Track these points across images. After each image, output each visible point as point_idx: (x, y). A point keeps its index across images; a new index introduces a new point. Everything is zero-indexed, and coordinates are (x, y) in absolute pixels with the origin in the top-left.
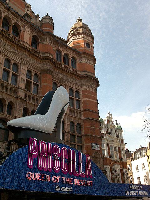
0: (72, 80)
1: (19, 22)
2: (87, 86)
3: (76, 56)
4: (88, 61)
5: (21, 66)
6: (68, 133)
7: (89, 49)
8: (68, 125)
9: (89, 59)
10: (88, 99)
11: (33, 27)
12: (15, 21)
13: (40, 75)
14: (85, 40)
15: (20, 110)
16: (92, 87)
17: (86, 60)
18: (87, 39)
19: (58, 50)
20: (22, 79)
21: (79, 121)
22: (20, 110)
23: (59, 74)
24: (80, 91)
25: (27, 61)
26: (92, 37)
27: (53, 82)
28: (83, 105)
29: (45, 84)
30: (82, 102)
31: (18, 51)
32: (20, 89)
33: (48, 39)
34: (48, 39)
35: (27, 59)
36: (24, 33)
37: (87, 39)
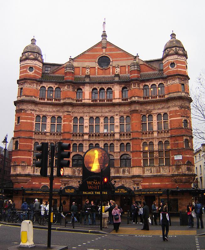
0: (159, 107)
1: (110, 86)
3: (163, 82)
6: (156, 151)
8: (156, 145)
11: (119, 83)
12: (107, 88)
13: (130, 116)
14: (170, 61)
15: (117, 147)
17: (171, 82)
19: (145, 85)
20: (116, 126)
21: (166, 139)
22: (117, 147)
23: (146, 108)
27: (142, 116)
29: (133, 122)
31: (111, 108)
32: (115, 134)
33: (133, 84)
34: (133, 84)
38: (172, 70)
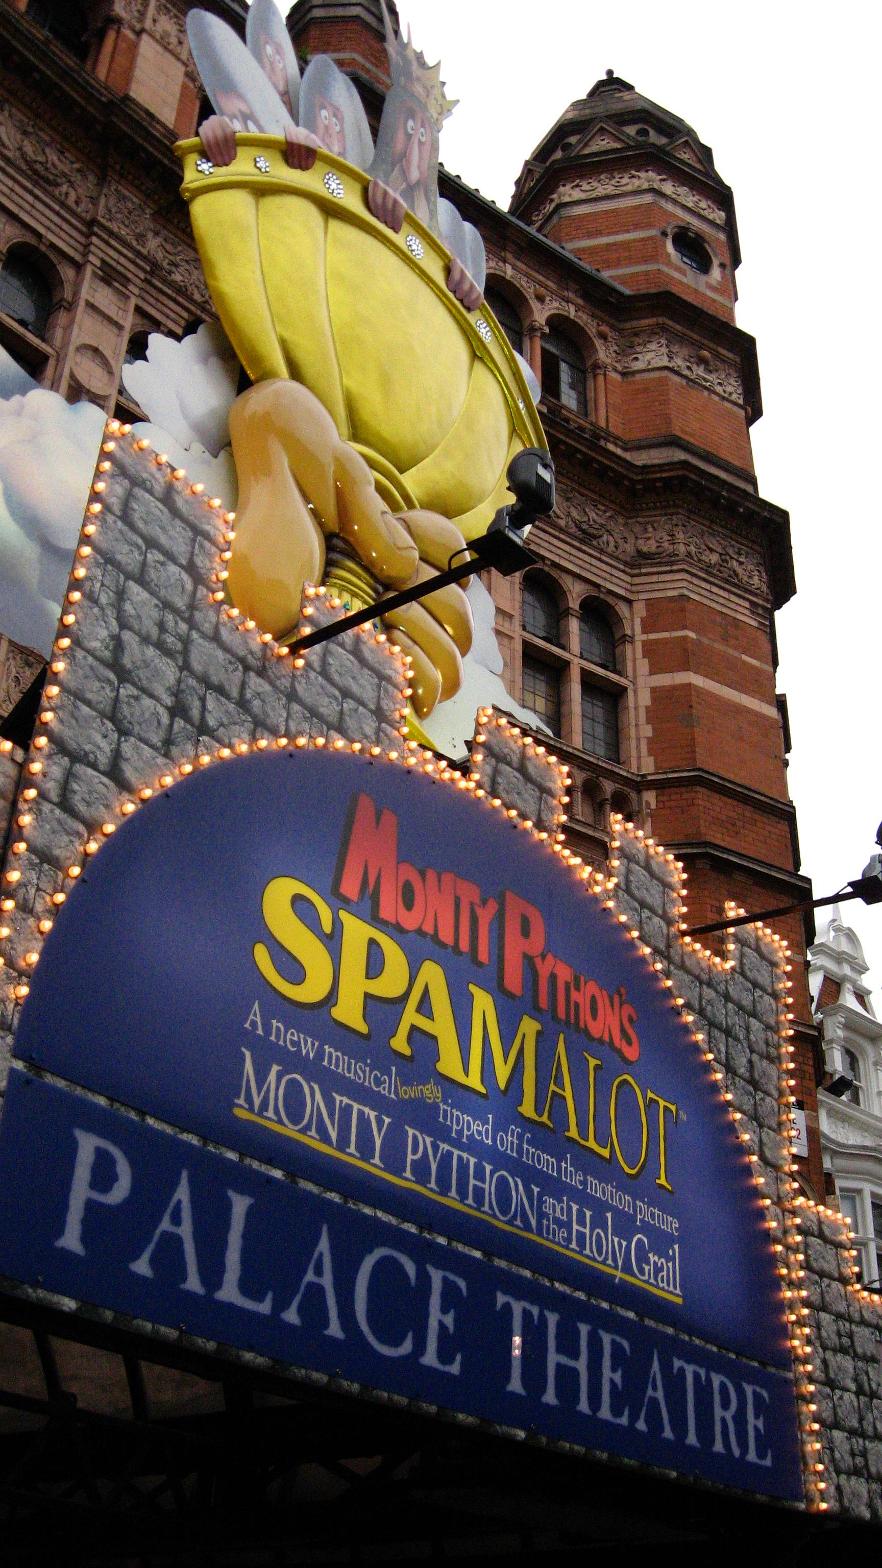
2: (687, 574)
4: (700, 371)
5: (77, 285)
7: (703, 278)
9: (706, 353)
10: (698, 680)
16: (732, 582)
18: (684, 207)
24: (622, 609)
25: (138, 254)
26: (723, 197)
28: (647, 731)
30: (645, 699)
35: (140, 237)
36: (134, 48)
37: (684, 207)
38: (685, 280)
